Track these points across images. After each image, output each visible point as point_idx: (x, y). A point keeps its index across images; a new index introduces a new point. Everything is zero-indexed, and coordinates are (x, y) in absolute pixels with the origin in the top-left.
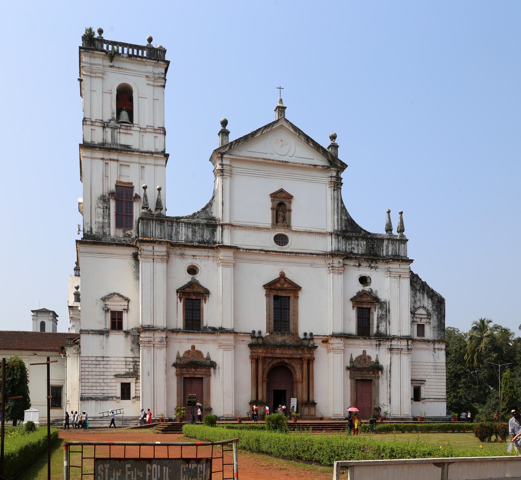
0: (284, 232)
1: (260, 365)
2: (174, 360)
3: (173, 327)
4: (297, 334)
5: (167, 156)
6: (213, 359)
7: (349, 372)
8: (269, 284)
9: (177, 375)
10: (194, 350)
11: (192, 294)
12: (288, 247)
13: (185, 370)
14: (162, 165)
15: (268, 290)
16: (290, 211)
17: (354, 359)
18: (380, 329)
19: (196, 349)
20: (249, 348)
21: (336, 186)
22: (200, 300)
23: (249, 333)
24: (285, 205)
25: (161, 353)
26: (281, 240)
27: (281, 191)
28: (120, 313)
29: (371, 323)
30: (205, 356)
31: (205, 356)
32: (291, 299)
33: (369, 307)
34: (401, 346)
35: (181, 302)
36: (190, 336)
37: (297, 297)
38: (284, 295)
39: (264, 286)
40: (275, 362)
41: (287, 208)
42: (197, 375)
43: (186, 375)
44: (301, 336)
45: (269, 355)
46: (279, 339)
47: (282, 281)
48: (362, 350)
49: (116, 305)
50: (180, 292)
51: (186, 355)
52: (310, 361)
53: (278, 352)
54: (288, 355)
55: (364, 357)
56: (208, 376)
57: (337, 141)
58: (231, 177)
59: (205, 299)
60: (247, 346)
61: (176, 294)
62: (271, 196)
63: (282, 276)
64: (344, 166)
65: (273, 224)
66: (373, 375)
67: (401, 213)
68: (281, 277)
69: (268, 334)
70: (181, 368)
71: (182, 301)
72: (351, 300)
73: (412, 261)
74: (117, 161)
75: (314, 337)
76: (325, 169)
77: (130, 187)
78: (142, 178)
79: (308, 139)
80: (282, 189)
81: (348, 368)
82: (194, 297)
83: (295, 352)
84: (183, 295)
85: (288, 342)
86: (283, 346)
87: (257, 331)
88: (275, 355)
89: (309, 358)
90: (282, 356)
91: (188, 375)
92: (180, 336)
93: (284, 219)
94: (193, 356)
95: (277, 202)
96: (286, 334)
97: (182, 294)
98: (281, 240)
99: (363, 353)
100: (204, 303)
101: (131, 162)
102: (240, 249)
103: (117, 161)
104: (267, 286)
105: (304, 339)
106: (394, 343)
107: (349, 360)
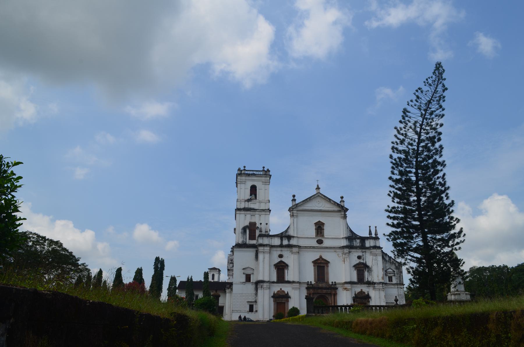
2: (272, 295)
3: (272, 281)
4: (329, 282)
5: (270, 211)
6: (290, 294)
9: (274, 301)
12: (323, 245)
14: (268, 214)
16: (323, 229)
18: (369, 279)
19: (282, 290)
22: (284, 269)
24: (320, 227)
25: (267, 292)
26: (320, 242)
27: (319, 222)
28: (250, 275)
29: (364, 276)
31: (286, 293)
32: (325, 267)
33: (362, 269)
35: (275, 269)
36: (280, 285)
37: (328, 266)
38: (322, 265)
39: (312, 262)
40: (318, 295)
41: (322, 228)
44: (331, 283)
45: (316, 292)
46: (320, 285)
47: (321, 259)
49: (248, 272)
52: (335, 295)
53: (319, 291)
55: (362, 292)
57: (343, 199)
58: (297, 217)
61: (273, 266)
63: (321, 257)
64: (347, 210)
65: (316, 236)
66: (366, 301)
67: (376, 227)
69: (315, 283)
72: (354, 266)
73: (382, 248)
74: (250, 214)
76: (339, 211)
77: (255, 224)
78: (260, 220)
79: (330, 200)
83: (328, 291)
85: (324, 286)
86: (322, 288)
87: (309, 282)
90: (322, 292)
92: (275, 285)
93: (321, 233)
94: (281, 293)
95: (317, 226)
98: (320, 242)
101: (255, 214)
102: (301, 246)
103: (250, 214)
106: (375, 285)
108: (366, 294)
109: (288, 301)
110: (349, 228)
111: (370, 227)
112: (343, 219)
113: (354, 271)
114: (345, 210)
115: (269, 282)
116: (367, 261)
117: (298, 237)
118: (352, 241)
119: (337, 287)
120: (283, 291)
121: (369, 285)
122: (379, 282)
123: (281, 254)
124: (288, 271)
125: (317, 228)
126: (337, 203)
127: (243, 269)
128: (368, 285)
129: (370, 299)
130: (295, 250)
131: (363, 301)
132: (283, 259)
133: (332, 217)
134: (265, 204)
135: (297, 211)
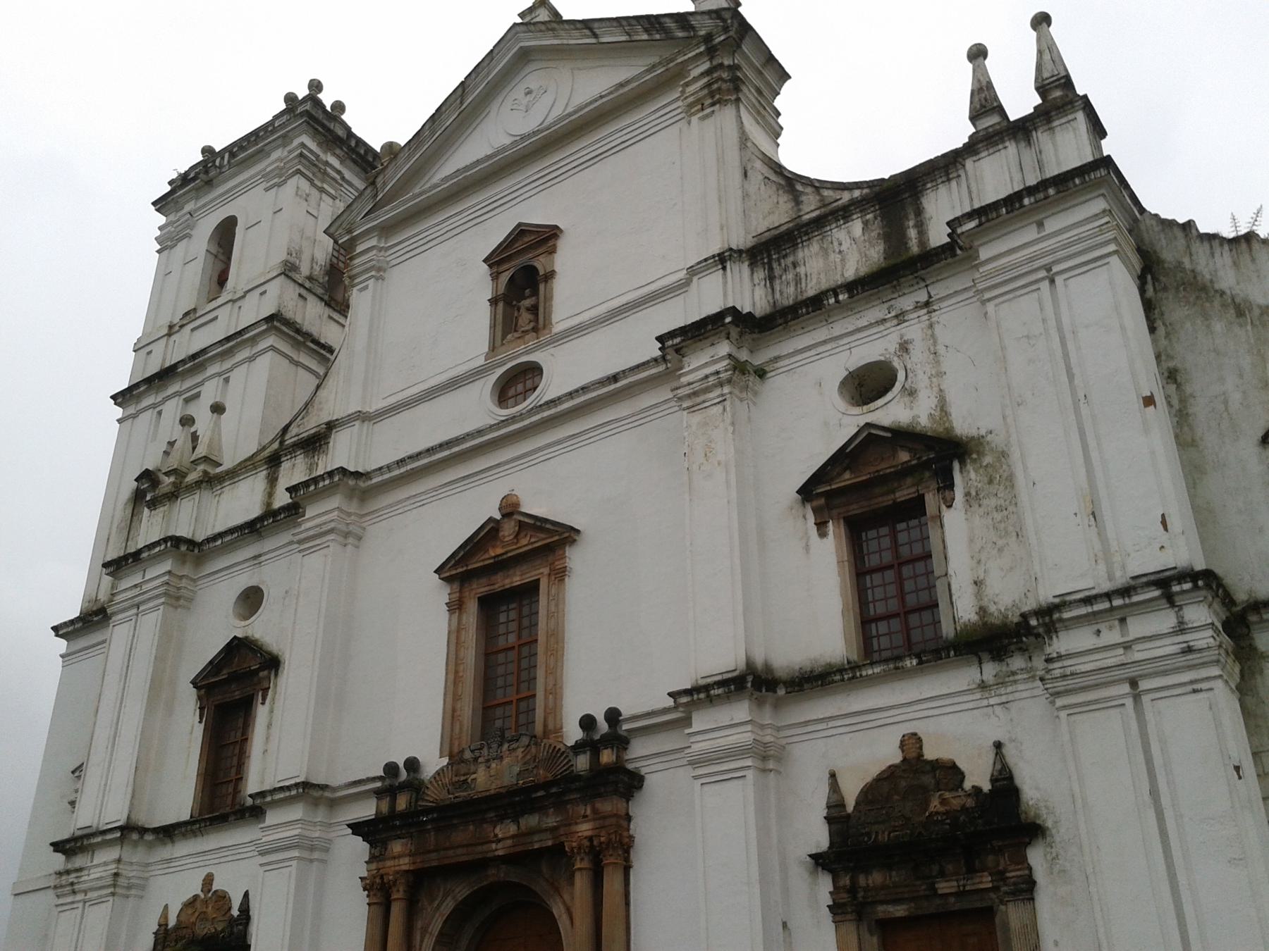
0: (527, 353)
1: (397, 910)
4: (559, 730)
7: (825, 885)
15: (456, 586)
16: (550, 275)
17: (851, 793)
21: (709, 101)
23: (374, 779)
27: (521, 231)
33: (904, 494)
34: (1127, 646)
35: (200, 722)
37: (560, 574)
40: (462, 891)
45: (433, 860)
46: (484, 780)
47: (508, 530)
48: (894, 736)
54: (500, 845)
62: (490, 266)
63: (510, 508)
66: (986, 881)
68: (504, 516)
72: (806, 492)
75: (625, 727)
80: (520, 225)
81: (819, 861)
83: (531, 821)
88: (451, 853)
89: (590, 839)
92: (183, 848)
97: (203, 692)
99: (903, 751)
104: (450, 569)
105: (578, 747)
106: (1064, 643)
107: (824, 813)
108: (968, 785)
110: (758, 164)
111: (978, 54)
112: (707, 116)
113: (807, 548)
114: (708, 38)
115: (129, 831)
116: (951, 396)
117: (362, 417)
118: (790, 259)
119: (630, 766)
121: (999, 654)
122: (1120, 580)
123: (253, 582)
124: (271, 711)
126: (638, 19)
127: (73, 772)
128: (990, 670)
129: (1036, 857)
130: (317, 513)
131: (944, 887)
132: (262, 628)
133: (624, 146)
134: (261, 294)
135: (387, 230)
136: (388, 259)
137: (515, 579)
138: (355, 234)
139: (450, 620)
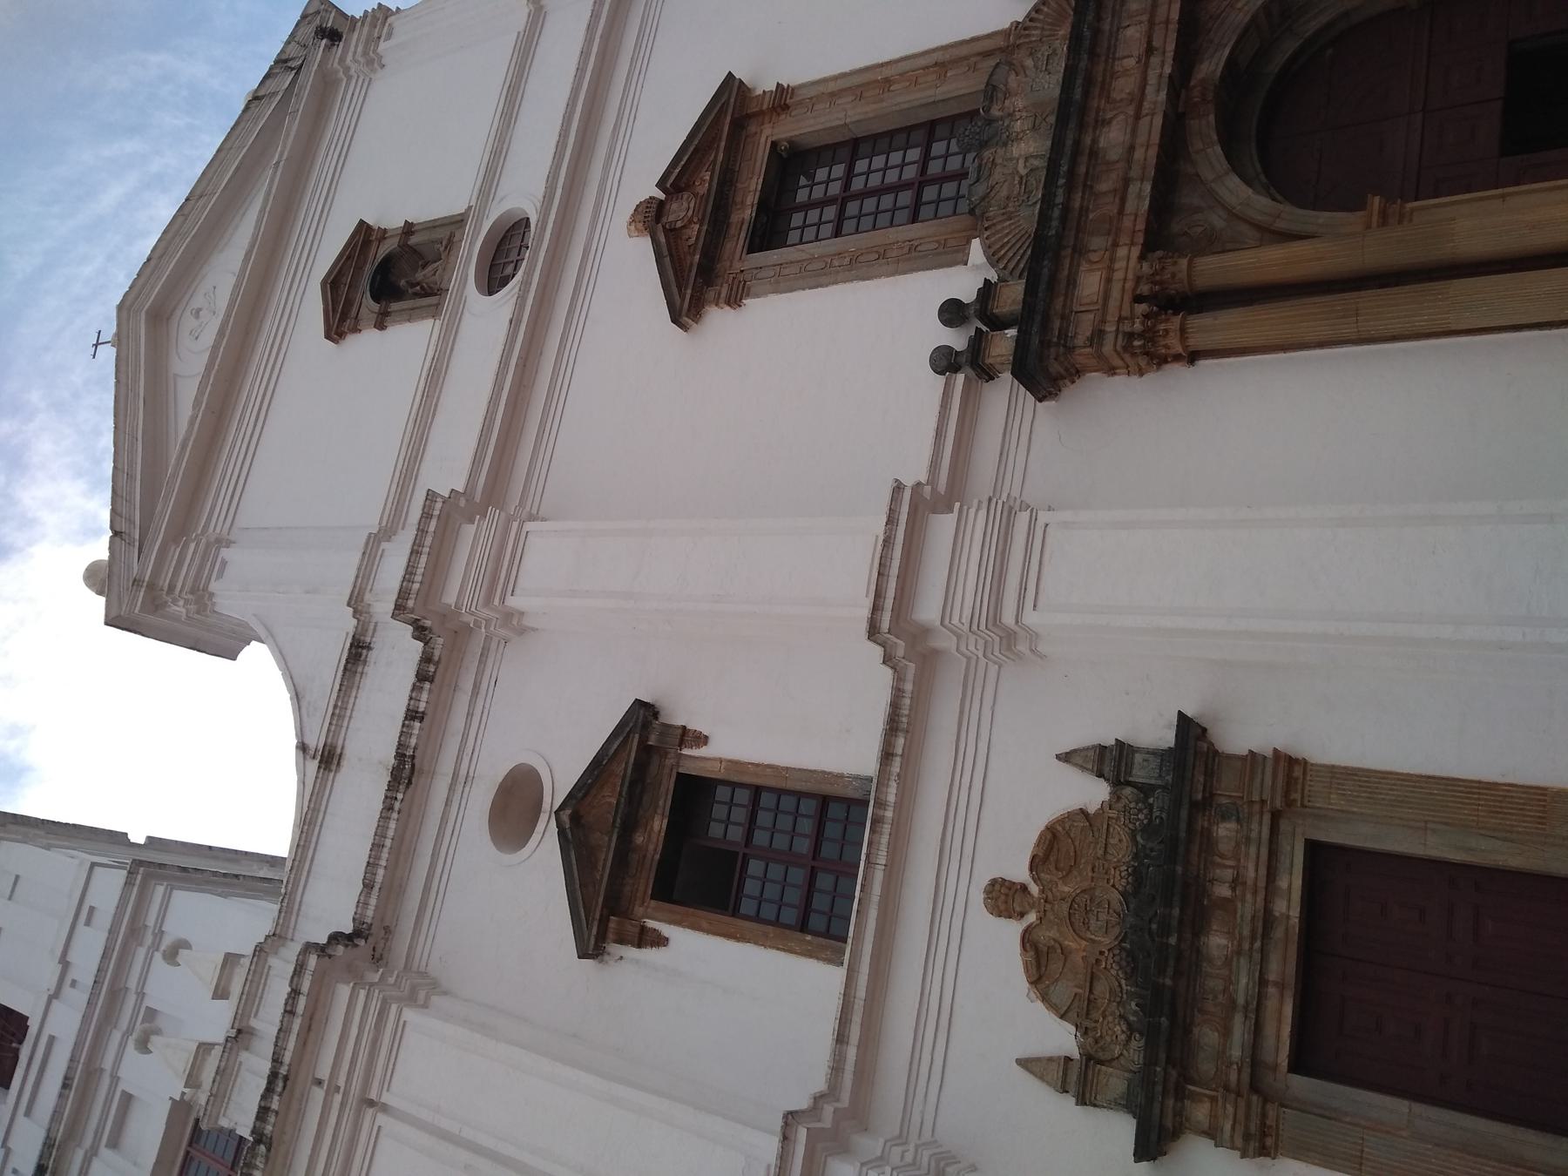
1: (1213, 269)
8: (675, 290)
10: (1024, 888)
11: (639, 839)
13: (1208, 1036)
16: (409, 229)
19: (1020, 872)
20: (1069, 391)
27: (334, 285)
30: (1093, 793)
31: (1093, 793)
32: (785, 129)
35: (660, 941)
37: (783, 99)
39: (675, 319)
40: (1209, 158)
42: (1280, 907)
43: (1269, 1029)
45: (1140, 197)
47: (680, 211)
50: (602, 938)
51: (1064, 991)
56: (1290, 782)
59: (689, 737)
60: (1049, 404)
69: (976, 248)
70: (1186, 1078)
71: (666, 929)
74: (93, 1152)
80: (324, 283)
82: (659, 824)
84: (626, 914)
88: (1139, 154)
90: (1157, 97)
91: (1271, 1004)
95: (369, 306)
96: (996, 112)
100: (702, 752)
101: (115, 1079)
109: (1289, 767)
120: (1036, 864)
125: (376, 307)
133: (344, 156)
134: (88, 923)
136: (218, 530)
137: (752, 187)
138: (147, 579)
139: (757, 296)
